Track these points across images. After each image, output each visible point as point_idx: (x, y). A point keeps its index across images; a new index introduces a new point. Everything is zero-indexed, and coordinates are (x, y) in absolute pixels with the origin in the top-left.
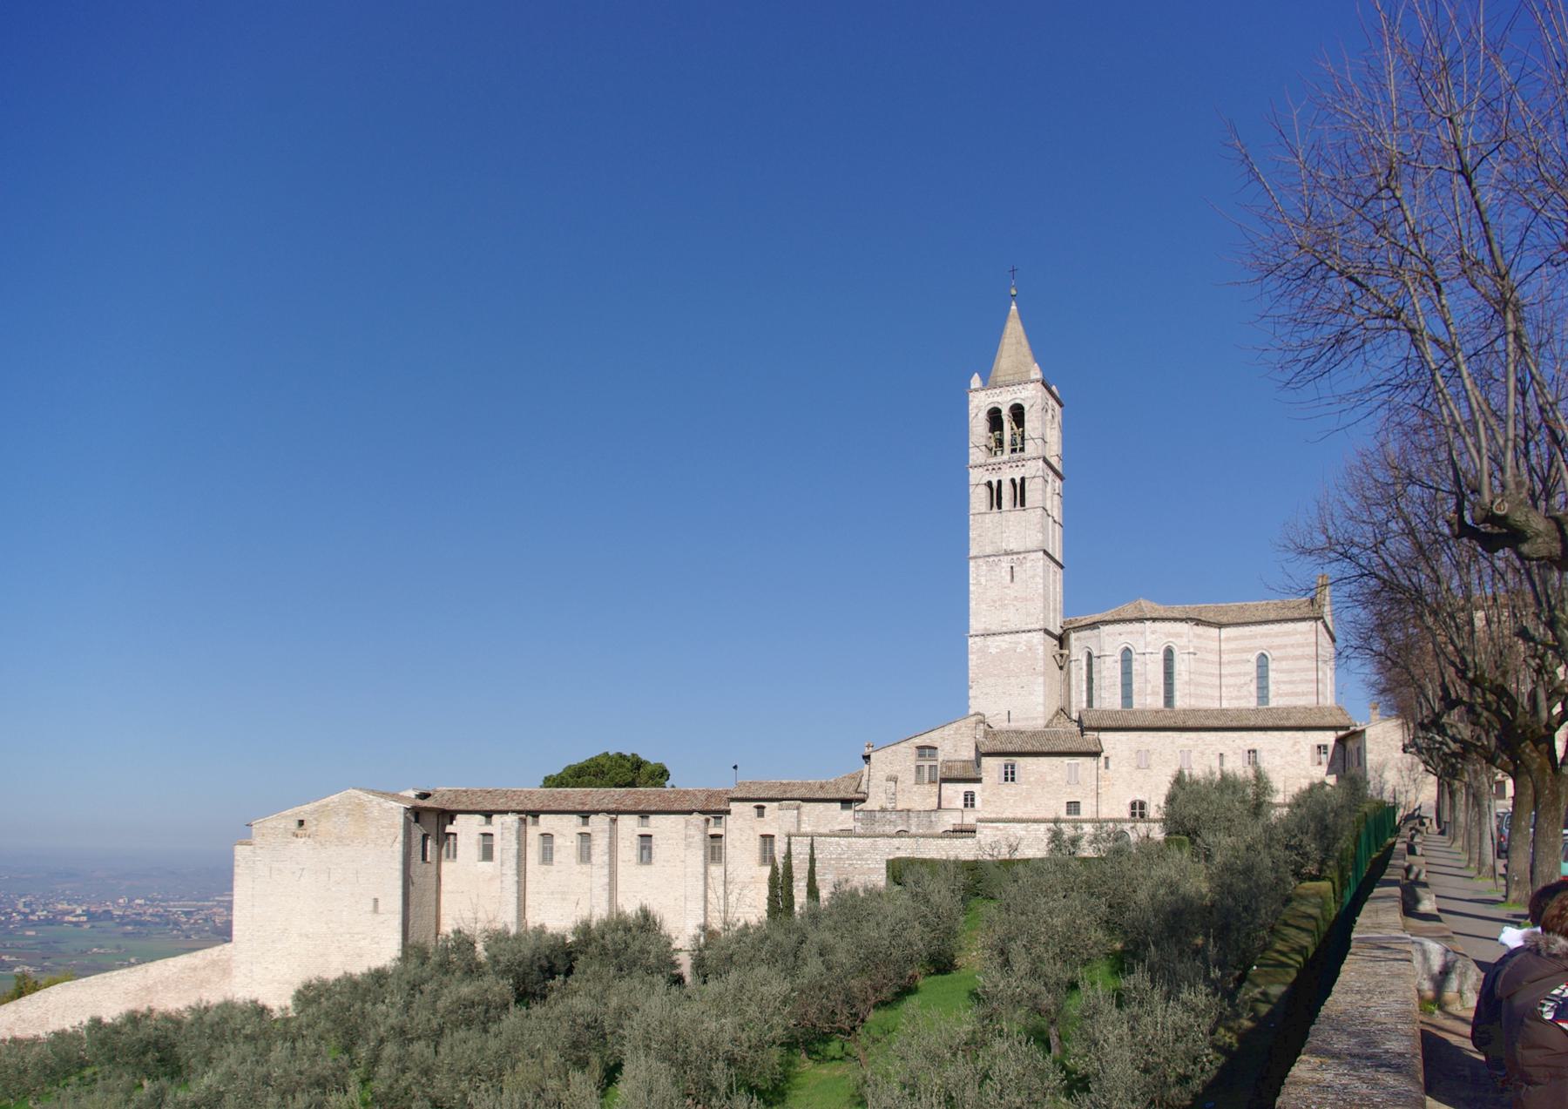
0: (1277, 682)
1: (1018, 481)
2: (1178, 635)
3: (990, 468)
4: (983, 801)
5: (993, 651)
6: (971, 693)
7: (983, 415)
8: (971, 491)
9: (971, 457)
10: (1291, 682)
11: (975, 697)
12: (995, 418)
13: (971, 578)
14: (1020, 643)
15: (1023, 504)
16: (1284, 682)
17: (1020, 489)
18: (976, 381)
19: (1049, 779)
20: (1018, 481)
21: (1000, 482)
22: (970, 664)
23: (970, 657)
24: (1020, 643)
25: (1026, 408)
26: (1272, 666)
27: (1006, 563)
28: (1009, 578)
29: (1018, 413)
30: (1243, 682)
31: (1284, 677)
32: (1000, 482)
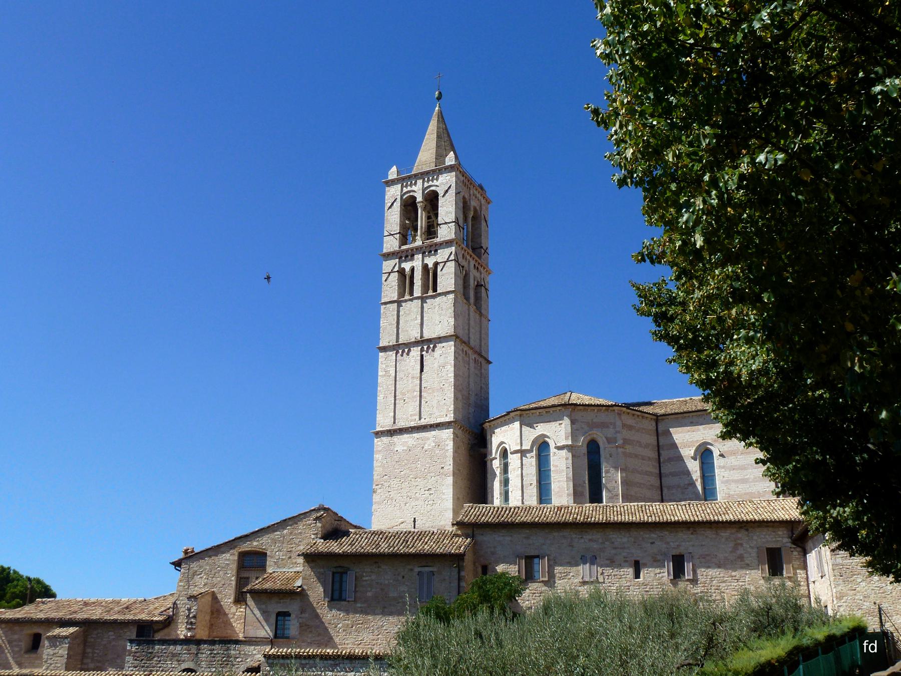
0: (727, 481)
1: (431, 265)
2: (603, 425)
3: (404, 255)
4: (301, 626)
5: (399, 448)
6: (376, 498)
7: (397, 205)
8: (384, 279)
9: (385, 245)
10: (744, 481)
11: (379, 503)
12: (409, 206)
13: (379, 370)
14: (428, 439)
15: (435, 290)
16: (737, 481)
17: (431, 276)
18: (393, 173)
19: (393, 594)
20: (431, 265)
21: (413, 270)
22: (376, 464)
23: (377, 456)
24: (428, 439)
25: (441, 193)
26: (717, 461)
27: (415, 352)
28: (419, 367)
29: (432, 199)
30: (686, 482)
31: (736, 475)
32: (413, 270)
